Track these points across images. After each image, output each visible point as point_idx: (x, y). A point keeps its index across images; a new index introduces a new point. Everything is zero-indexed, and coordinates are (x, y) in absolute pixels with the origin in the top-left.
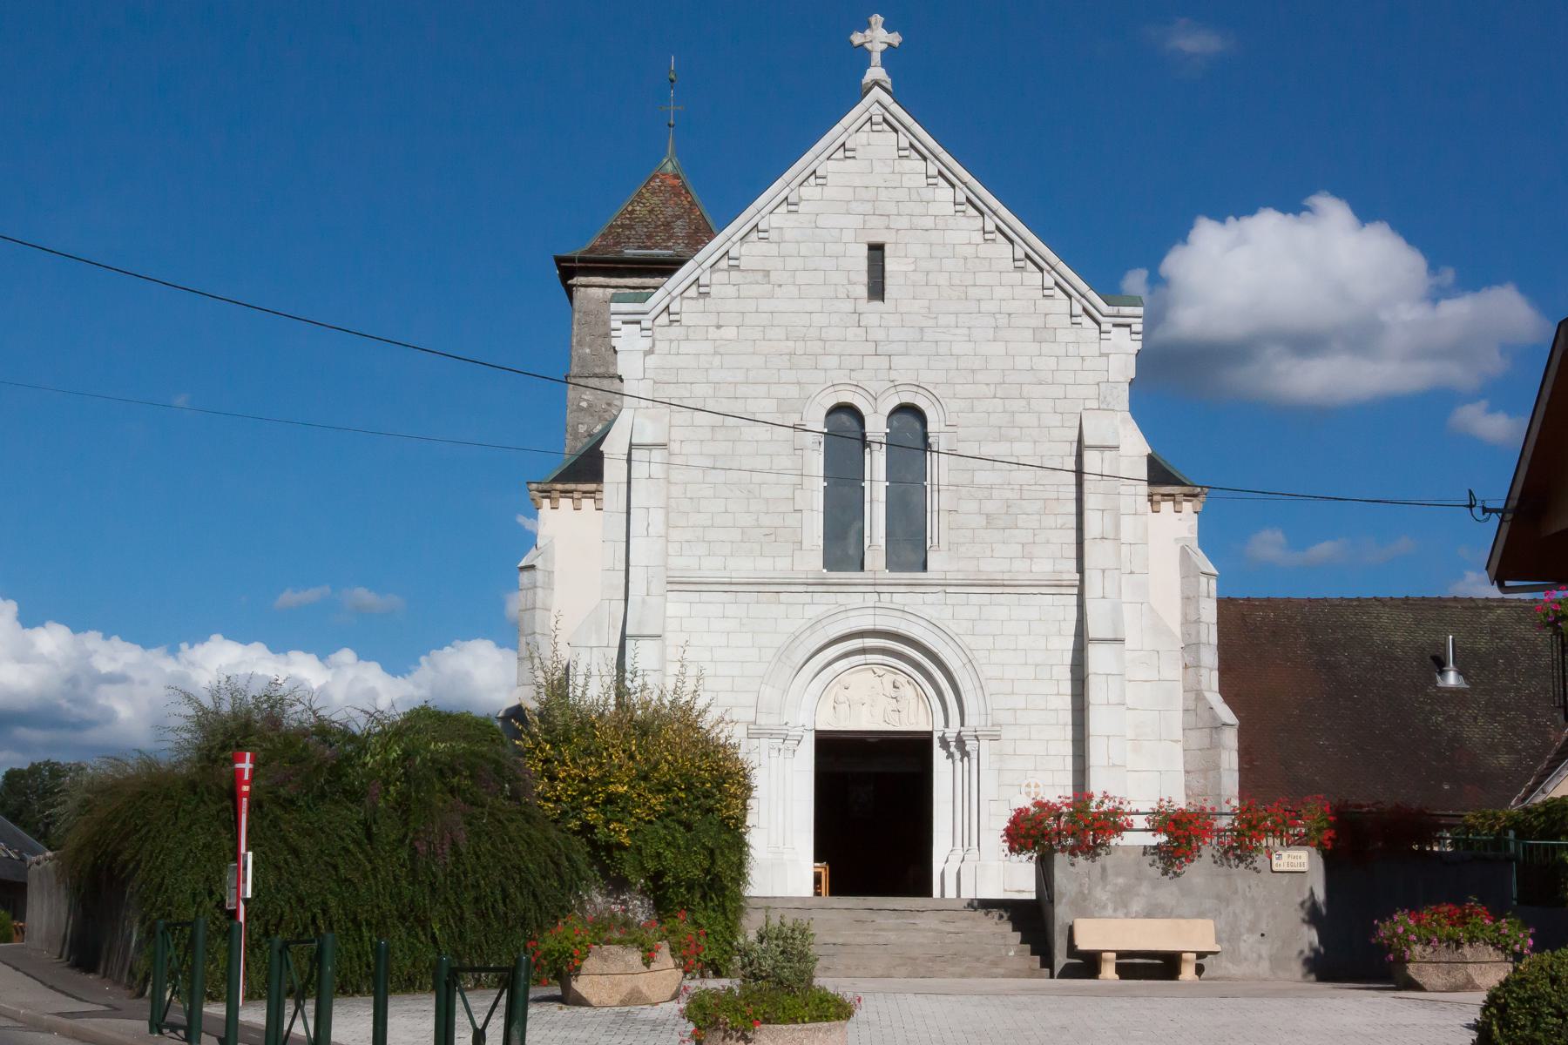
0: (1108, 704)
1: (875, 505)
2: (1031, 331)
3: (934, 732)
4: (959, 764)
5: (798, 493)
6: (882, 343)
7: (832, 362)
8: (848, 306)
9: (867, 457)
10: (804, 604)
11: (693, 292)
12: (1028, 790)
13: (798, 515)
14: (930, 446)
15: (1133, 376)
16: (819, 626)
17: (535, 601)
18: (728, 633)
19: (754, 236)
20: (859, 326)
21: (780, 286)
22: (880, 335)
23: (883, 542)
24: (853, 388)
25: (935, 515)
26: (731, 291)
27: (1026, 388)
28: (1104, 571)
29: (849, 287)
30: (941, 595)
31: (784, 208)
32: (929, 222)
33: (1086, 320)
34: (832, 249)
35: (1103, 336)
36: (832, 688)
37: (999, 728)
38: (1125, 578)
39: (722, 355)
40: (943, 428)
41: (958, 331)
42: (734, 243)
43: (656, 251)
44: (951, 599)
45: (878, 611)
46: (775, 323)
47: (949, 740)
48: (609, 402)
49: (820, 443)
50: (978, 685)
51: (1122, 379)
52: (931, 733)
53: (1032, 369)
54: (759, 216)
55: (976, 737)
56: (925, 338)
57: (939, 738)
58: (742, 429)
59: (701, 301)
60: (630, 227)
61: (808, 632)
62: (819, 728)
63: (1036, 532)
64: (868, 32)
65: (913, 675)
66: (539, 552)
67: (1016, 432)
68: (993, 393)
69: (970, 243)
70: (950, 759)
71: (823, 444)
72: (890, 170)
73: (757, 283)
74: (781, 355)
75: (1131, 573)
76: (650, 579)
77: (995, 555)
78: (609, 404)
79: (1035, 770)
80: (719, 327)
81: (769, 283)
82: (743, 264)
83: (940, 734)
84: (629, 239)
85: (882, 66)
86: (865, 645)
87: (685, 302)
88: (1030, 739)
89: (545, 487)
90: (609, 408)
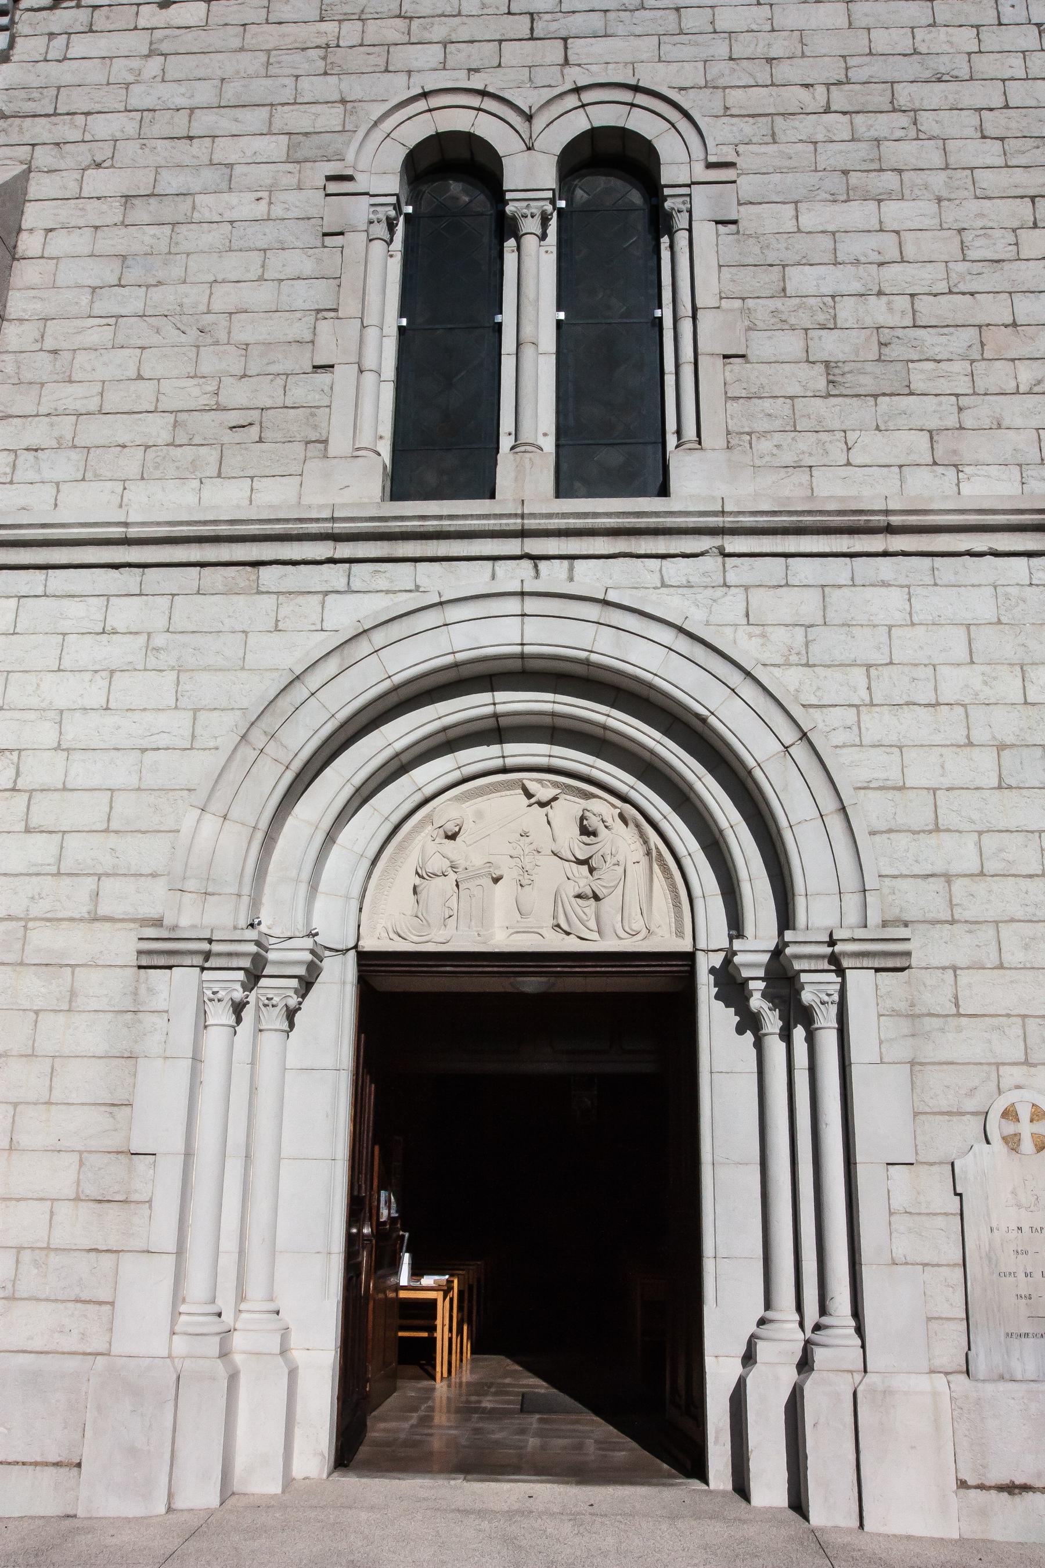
1: (528, 351)
3: (701, 958)
4: (776, 1049)
9: (510, 259)
10: (326, 593)
12: (1010, 1128)
13: (323, 378)
14: (669, 216)
16: (364, 647)
18: (112, 672)
23: (549, 444)
24: (475, 101)
25: (687, 371)
30: (712, 563)
37: (901, 932)
39: (165, 55)
40: (700, 172)
44: (740, 571)
45: (532, 605)
47: (745, 973)
49: (391, 226)
50: (828, 804)
52: (689, 958)
53: (916, 52)
55: (834, 959)
57: (712, 971)
58: (199, 198)
61: (332, 666)
62: (368, 944)
63: (964, 401)
65: (634, 795)
67: (890, 180)
68: (823, 102)
70: (749, 1036)
74: (303, 49)
77: (856, 460)
79: (1026, 1063)
83: (717, 960)
86: (501, 708)
88: (1001, 966)
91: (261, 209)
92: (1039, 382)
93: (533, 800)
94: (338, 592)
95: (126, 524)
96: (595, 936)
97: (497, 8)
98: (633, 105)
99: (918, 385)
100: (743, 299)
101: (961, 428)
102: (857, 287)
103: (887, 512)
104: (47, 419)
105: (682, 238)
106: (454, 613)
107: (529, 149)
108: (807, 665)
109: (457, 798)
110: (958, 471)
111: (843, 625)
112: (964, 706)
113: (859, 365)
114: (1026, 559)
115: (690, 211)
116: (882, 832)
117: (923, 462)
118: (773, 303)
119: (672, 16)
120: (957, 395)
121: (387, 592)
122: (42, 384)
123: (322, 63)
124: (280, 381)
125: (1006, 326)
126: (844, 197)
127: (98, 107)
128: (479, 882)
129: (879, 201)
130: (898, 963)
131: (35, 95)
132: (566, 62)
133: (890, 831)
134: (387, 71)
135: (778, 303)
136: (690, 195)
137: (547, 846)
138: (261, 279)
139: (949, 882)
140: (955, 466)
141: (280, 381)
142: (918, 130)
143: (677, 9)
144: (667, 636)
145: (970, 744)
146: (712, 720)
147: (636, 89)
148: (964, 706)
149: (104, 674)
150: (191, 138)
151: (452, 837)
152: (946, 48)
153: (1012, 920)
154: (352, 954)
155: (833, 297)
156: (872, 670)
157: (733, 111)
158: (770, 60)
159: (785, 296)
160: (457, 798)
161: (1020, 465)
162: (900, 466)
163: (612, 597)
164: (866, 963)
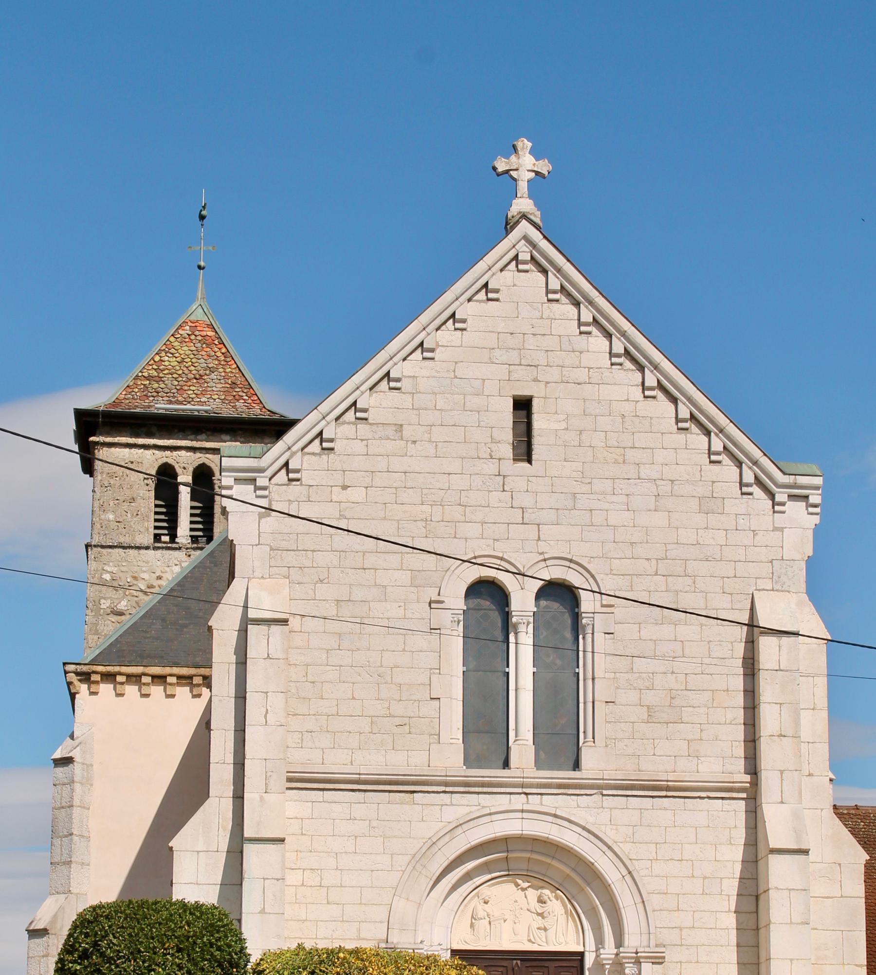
0: (791, 923)
2: (697, 500)
5: (434, 678)
6: (530, 511)
7: (472, 530)
8: (491, 467)
10: (442, 805)
11: (315, 446)
15: (811, 554)
17: (72, 797)
19: (384, 384)
20: (504, 491)
21: (414, 442)
22: (527, 501)
23: (530, 736)
25: (590, 705)
26: (359, 447)
27: (691, 565)
28: (782, 772)
29: (494, 447)
30: (597, 798)
31: (418, 354)
32: (581, 375)
33: (755, 490)
34: (474, 402)
35: (777, 508)
36: (469, 902)
38: (805, 779)
39: (348, 519)
40: (599, 609)
41: (615, 498)
42: (363, 393)
43: (189, 407)
44: (609, 802)
45: (525, 815)
46: (409, 485)
47: (605, 962)
48: (136, 575)
50: (638, 900)
51: (797, 556)
52: (581, 954)
54: (391, 363)
56: (578, 506)
58: (372, 604)
59: (325, 457)
60: (160, 379)
61: (447, 838)
64: (513, 158)
66: (77, 742)
69: (628, 400)
71: (462, 623)
72: (539, 314)
73: (389, 439)
74: (415, 521)
75: (810, 775)
76: (269, 774)
78: (135, 578)
80: (345, 487)
81: (402, 439)
82: (371, 415)
84: (158, 393)
85: (530, 197)
87: (306, 457)
88: (698, 962)
89: (85, 669)
90: (135, 582)
91: (401, 613)
92: (735, 719)
93: (519, 887)
94: (447, 805)
95: (359, 774)
96: (545, 944)
97: (506, 503)
98: (569, 567)
99: (685, 719)
100: (615, 673)
101: (701, 740)
102: (663, 669)
103: (667, 781)
104: (314, 717)
105: (589, 637)
106: (494, 817)
107: (522, 589)
108: (633, 842)
109: (489, 886)
110: (698, 759)
111: (648, 826)
112: (692, 861)
113: (662, 708)
114: (721, 801)
115: (593, 625)
116: (657, 911)
117: (684, 755)
118: (627, 676)
119: (588, 514)
120: (701, 724)
121: (467, 806)
122: (310, 699)
123: (424, 530)
124: (416, 704)
125: (724, 691)
126: (661, 622)
127: (318, 548)
128: (499, 922)
129: (676, 625)
130: (660, 961)
131: (286, 537)
132: (539, 539)
133: (661, 910)
134: (455, 537)
135: (629, 676)
136: (593, 618)
137: (525, 906)
138: (404, 650)
139: (681, 930)
140: (697, 757)
141: (416, 704)
142: (695, 587)
143: (591, 510)
144: (579, 830)
145: (693, 876)
146: (596, 864)
147: (571, 561)
148: (692, 861)
149: (353, 838)
150: (365, 569)
151: (486, 902)
152: (712, 542)
153: (703, 945)
154: (450, 950)
155: (653, 673)
156: (658, 845)
157: (614, 572)
158: (632, 543)
159: (633, 672)
160: (489, 886)
161: (723, 758)
162: (675, 756)
163: (559, 813)
164: (648, 960)
